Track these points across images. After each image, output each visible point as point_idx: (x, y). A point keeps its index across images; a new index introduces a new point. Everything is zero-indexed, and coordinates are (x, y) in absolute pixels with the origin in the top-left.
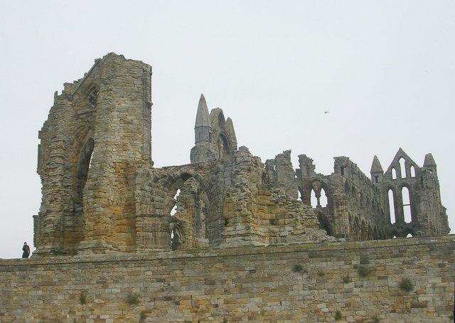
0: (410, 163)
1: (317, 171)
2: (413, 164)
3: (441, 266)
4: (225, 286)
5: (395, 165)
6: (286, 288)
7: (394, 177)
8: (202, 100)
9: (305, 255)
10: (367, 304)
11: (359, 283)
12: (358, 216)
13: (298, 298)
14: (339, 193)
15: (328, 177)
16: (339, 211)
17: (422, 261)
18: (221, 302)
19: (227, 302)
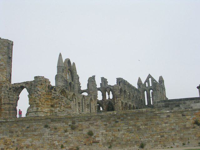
0: (153, 80)
1: (109, 84)
2: (155, 80)
3: (106, 125)
4: (17, 134)
5: (147, 81)
6: (41, 135)
7: (147, 86)
8: (60, 55)
9: (49, 121)
10: (74, 141)
11: (71, 132)
12: (127, 102)
13: (46, 139)
14: (117, 93)
15: (113, 86)
16: (117, 100)
17: (98, 123)
18: (15, 140)
19: (18, 140)
